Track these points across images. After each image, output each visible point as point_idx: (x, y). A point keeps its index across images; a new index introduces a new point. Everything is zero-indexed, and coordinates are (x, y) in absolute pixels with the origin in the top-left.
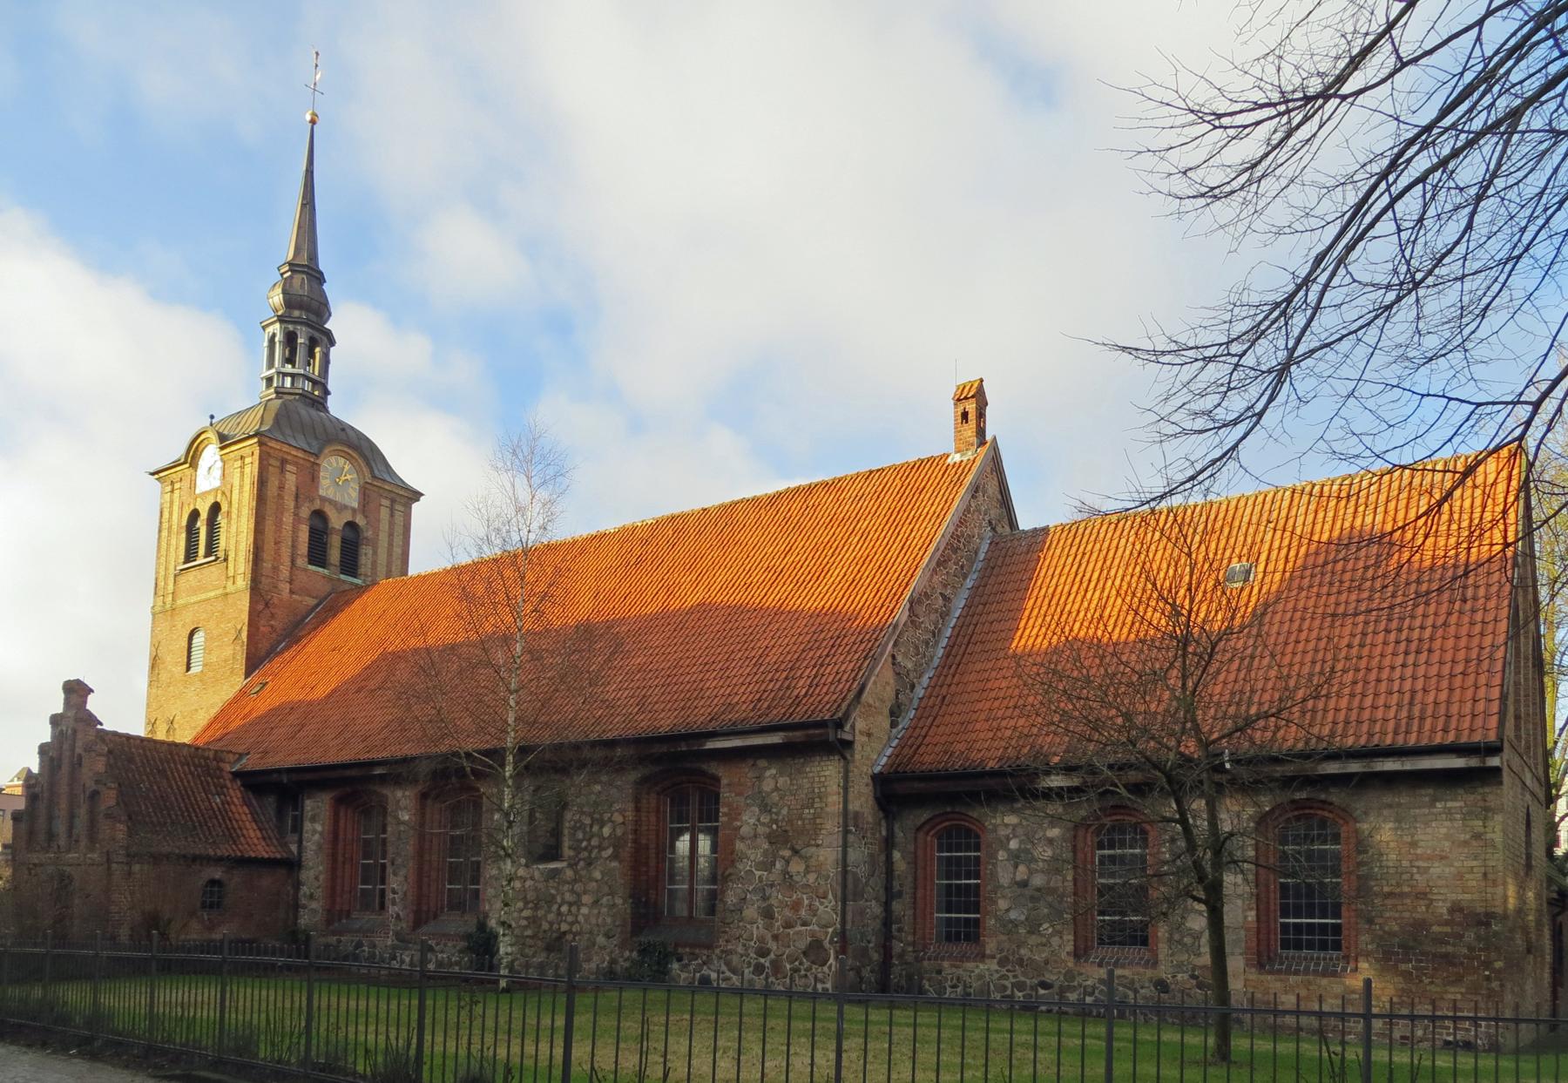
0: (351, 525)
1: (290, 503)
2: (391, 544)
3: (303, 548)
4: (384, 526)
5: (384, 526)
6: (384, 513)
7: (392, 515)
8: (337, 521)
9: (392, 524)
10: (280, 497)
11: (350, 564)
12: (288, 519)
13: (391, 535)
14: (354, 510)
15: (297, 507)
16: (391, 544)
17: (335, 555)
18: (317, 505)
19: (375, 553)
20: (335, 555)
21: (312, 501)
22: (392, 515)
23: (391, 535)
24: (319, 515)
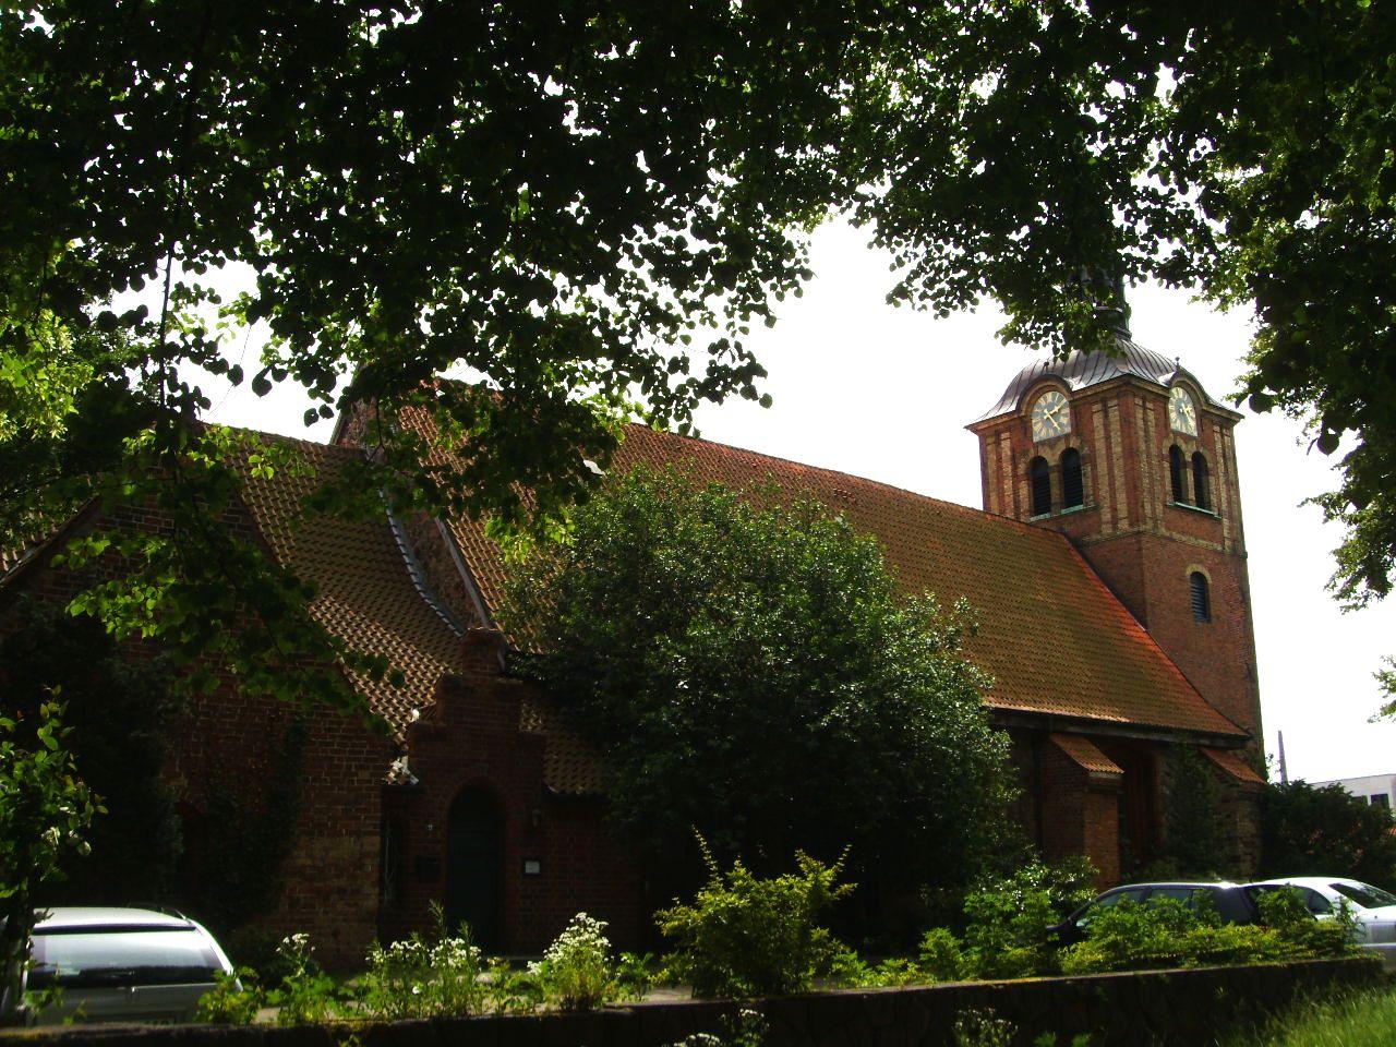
0: (1069, 453)
1: (1008, 469)
2: (1109, 448)
3: (1025, 505)
4: (1099, 434)
5: (1099, 434)
6: (1098, 420)
7: (1106, 416)
8: (1052, 457)
9: (1106, 426)
10: (1000, 468)
11: (1073, 493)
12: (1008, 485)
13: (1108, 438)
14: (1067, 436)
15: (1015, 468)
16: (1109, 448)
17: (1056, 492)
18: (1032, 454)
19: (1094, 467)
20: (1056, 492)
21: (1025, 453)
22: (1106, 416)
23: (1108, 438)
24: (1039, 461)
